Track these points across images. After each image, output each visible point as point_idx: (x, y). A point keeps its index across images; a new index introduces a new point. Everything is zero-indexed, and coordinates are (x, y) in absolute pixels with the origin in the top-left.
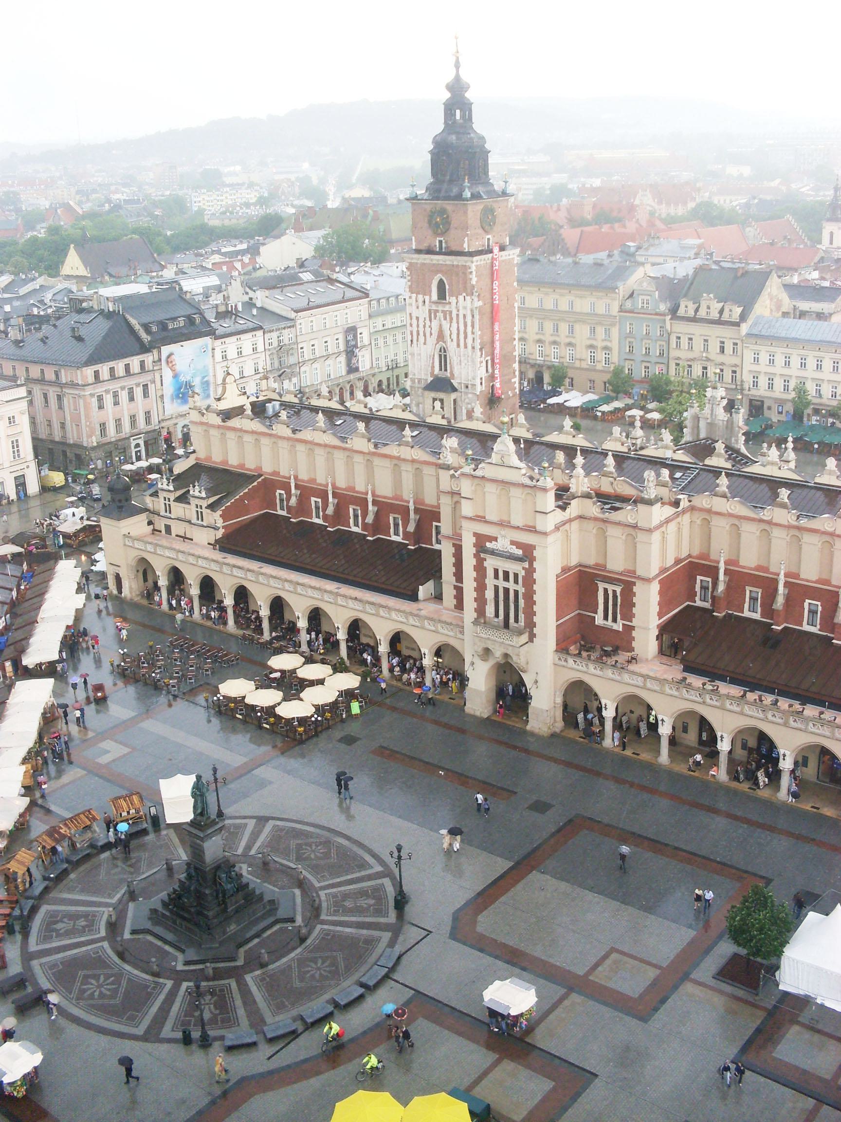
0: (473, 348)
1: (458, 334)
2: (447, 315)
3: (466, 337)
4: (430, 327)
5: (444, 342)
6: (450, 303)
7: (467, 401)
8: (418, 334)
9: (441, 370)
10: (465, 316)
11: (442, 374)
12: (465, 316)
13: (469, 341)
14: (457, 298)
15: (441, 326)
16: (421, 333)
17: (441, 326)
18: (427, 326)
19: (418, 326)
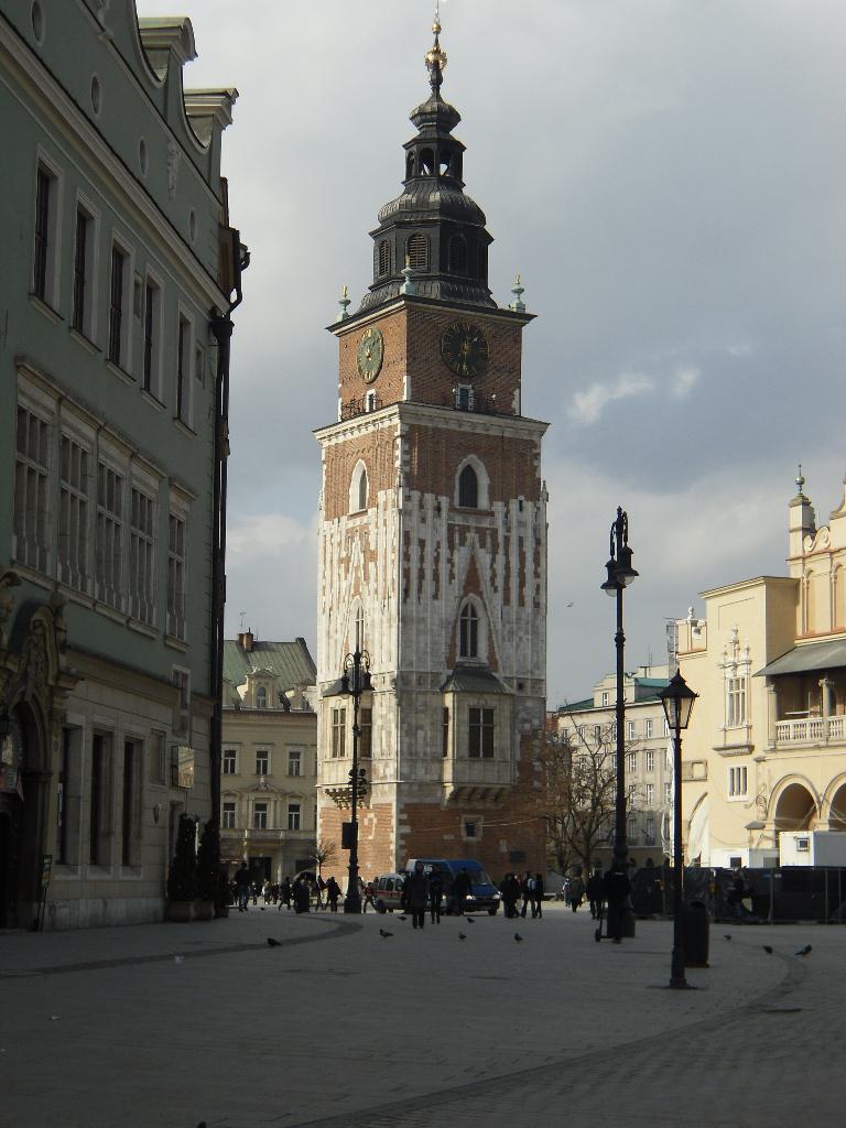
0: (537, 605)
1: (507, 578)
2: (488, 538)
3: (522, 584)
4: (450, 561)
5: (480, 594)
6: (492, 514)
7: (523, 715)
8: (421, 576)
9: (463, 653)
10: (521, 540)
11: (468, 661)
12: (521, 540)
13: (529, 592)
14: (507, 505)
15: (473, 560)
16: (429, 574)
17: (473, 560)
18: (443, 559)
19: (422, 559)
